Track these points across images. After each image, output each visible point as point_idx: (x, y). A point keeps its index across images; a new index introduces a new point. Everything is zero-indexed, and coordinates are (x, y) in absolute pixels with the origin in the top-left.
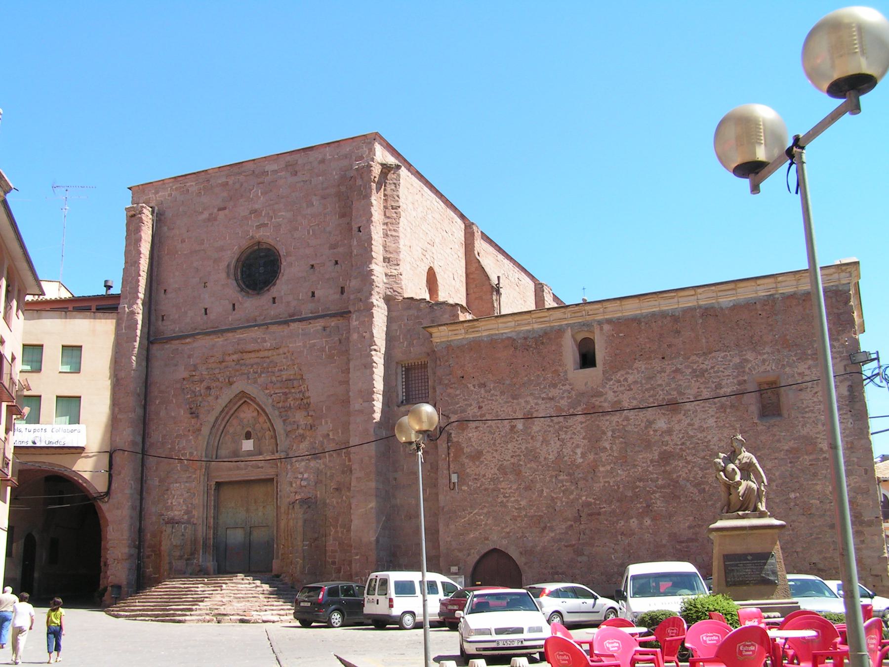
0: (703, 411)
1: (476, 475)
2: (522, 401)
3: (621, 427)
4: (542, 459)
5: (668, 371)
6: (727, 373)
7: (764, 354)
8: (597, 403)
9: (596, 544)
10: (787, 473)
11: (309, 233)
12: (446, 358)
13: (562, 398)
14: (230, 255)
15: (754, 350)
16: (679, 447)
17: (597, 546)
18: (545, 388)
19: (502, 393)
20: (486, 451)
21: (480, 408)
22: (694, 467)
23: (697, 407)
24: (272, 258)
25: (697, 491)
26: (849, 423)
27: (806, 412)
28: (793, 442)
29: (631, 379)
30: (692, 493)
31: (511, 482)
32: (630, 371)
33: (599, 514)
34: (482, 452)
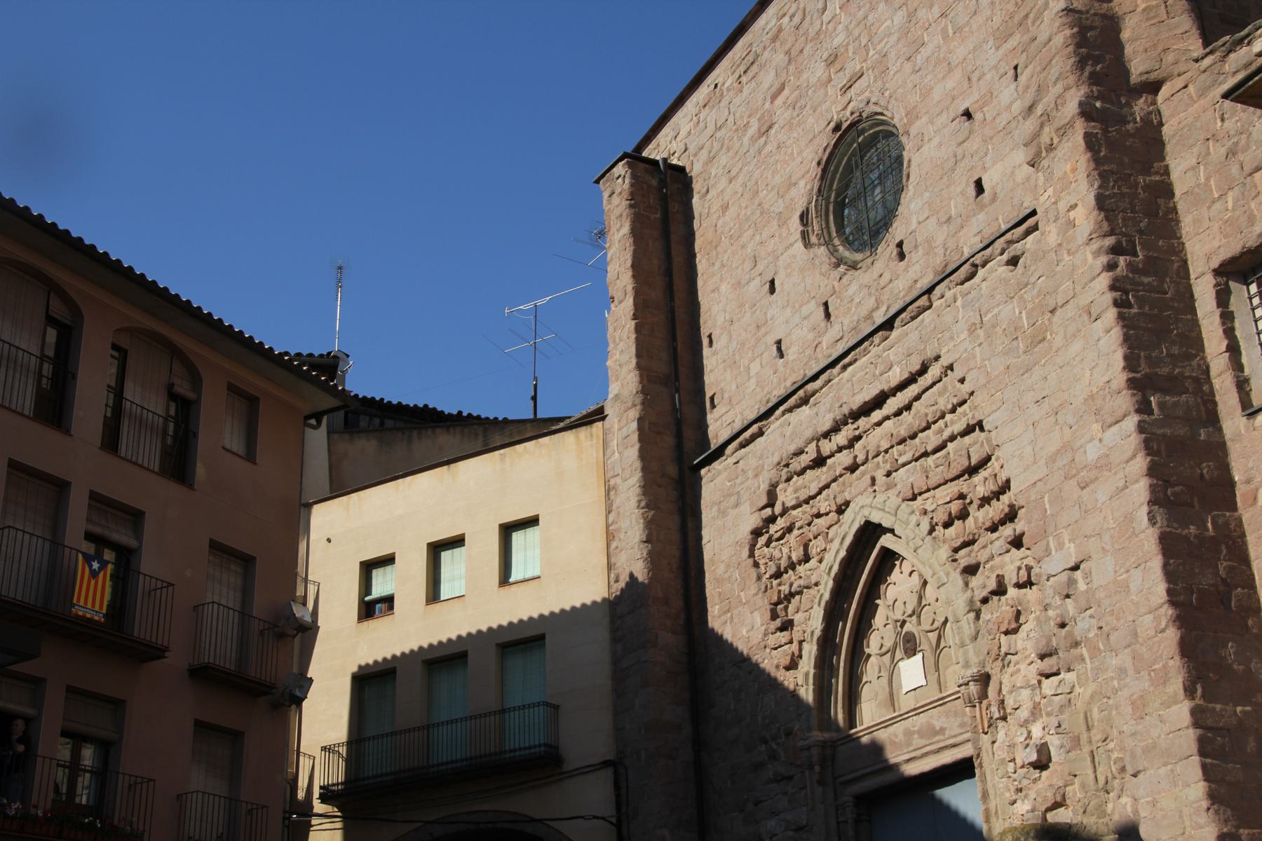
11: (944, 30)
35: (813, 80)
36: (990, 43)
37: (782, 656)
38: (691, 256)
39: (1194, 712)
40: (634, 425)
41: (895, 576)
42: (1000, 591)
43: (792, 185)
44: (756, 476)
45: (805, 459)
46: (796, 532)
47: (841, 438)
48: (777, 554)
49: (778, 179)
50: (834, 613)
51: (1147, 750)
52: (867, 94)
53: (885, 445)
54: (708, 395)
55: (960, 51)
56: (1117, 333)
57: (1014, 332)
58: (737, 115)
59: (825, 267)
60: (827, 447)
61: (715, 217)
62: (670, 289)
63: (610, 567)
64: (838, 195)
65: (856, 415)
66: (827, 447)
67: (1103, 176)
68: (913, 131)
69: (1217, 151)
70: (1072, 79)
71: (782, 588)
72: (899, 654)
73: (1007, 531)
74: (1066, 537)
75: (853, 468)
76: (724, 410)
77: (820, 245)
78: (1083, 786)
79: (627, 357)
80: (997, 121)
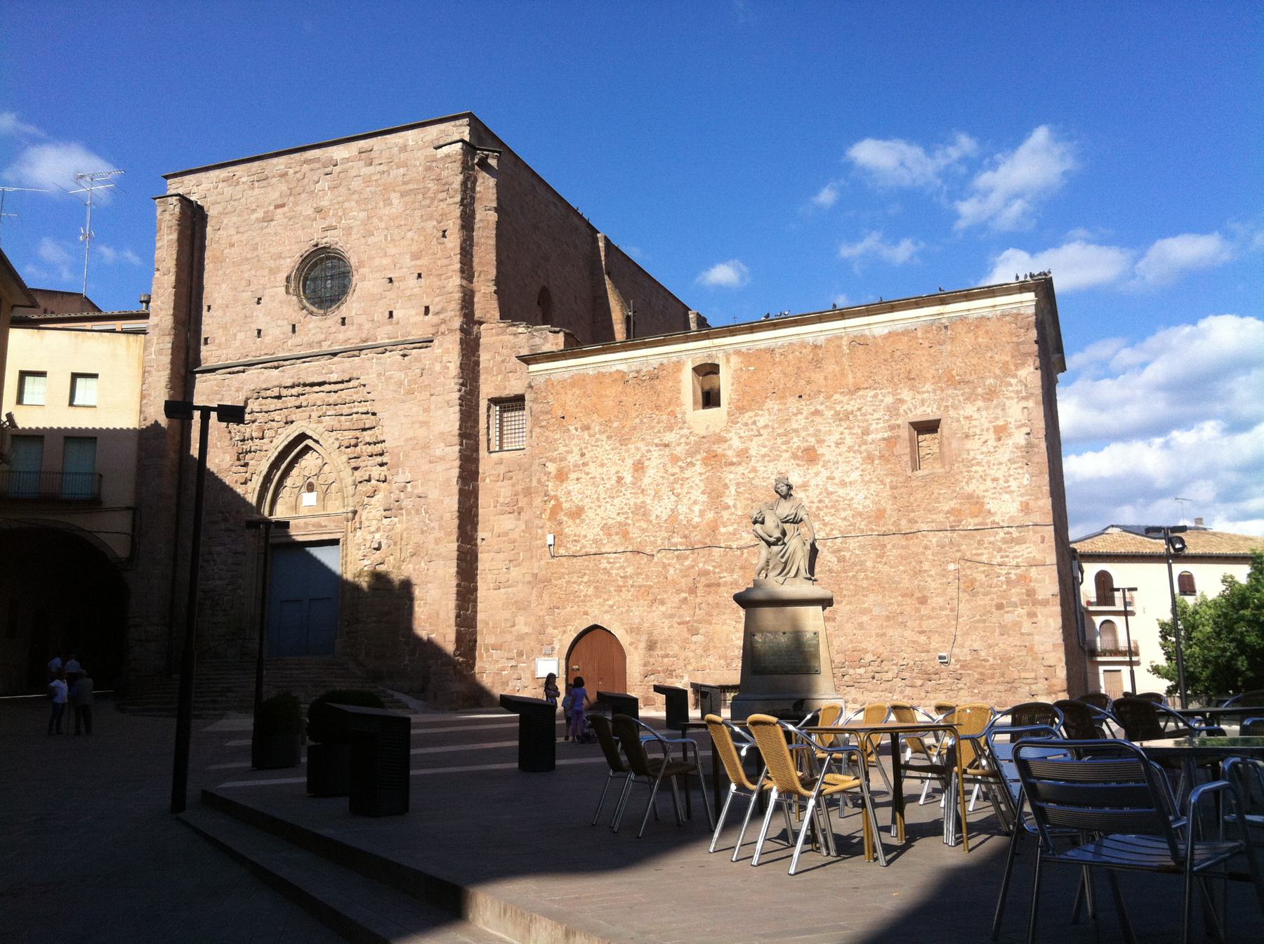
0: (846, 462)
1: (575, 535)
2: (631, 446)
3: (748, 479)
4: (653, 518)
5: (805, 414)
6: (876, 416)
7: (923, 392)
8: (719, 451)
9: (714, 621)
10: (947, 541)
11: (386, 239)
12: (544, 394)
13: (679, 444)
14: (289, 264)
15: (912, 388)
16: (816, 505)
17: (715, 623)
18: (659, 432)
19: (609, 438)
20: (588, 507)
21: (583, 455)
22: (832, 530)
23: (839, 458)
24: (342, 269)
25: (836, 559)
26: (1025, 479)
27: (973, 465)
28: (954, 501)
29: (762, 422)
30: (829, 561)
31: (616, 545)
32: (760, 412)
33: (718, 585)
34: (583, 508)
35: (305, 213)
36: (408, 257)
37: (241, 478)
38: (202, 259)
39: (458, 546)
40: (170, 345)
41: (308, 456)
42: (369, 480)
43: (280, 256)
44: (237, 391)
45: (268, 393)
46: (256, 424)
47: (295, 391)
48: (243, 430)
49: (273, 250)
50: (275, 466)
51: (436, 555)
52: (337, 239)
53: (319, 403)
54: (203, 336)
55: (392, 250)
56: (458, 416)
57: (400, 384)
58: (249, 201)
59: (296, 308)
60: (284, 392)
61: (224, 246)
62: (191, 274)
63: (141, 412)
64: (306, 274)
65: (305, 385)
66: (284, 392)
67: (463, 355)
68: (362, 271)
69: (499, 358)
70: (458, 313)
71: (244, 447)
72: (303, 489)
73: (379, 459)
74: (407, 470)
75: (298, 407)
76: (214, 348)
77: (294, 295)
78: (395, 559)
79: (167, 307)
80: (405, 292)
